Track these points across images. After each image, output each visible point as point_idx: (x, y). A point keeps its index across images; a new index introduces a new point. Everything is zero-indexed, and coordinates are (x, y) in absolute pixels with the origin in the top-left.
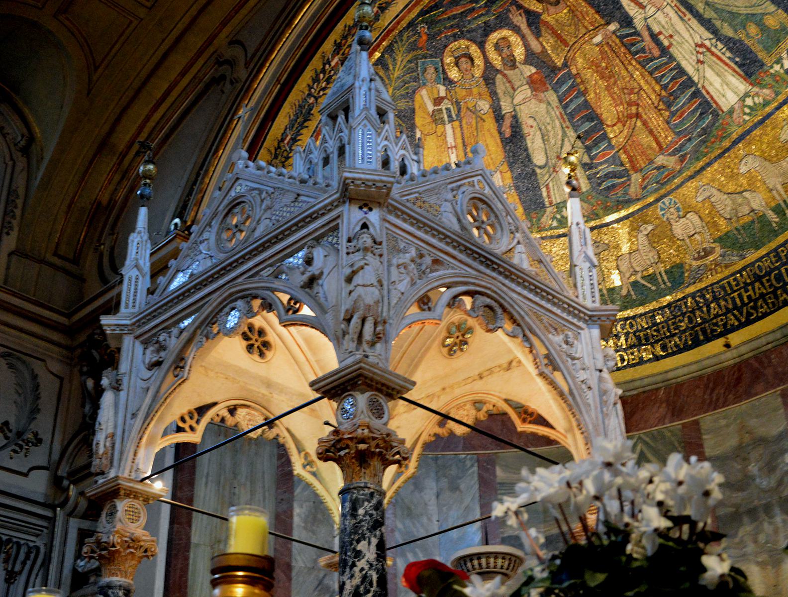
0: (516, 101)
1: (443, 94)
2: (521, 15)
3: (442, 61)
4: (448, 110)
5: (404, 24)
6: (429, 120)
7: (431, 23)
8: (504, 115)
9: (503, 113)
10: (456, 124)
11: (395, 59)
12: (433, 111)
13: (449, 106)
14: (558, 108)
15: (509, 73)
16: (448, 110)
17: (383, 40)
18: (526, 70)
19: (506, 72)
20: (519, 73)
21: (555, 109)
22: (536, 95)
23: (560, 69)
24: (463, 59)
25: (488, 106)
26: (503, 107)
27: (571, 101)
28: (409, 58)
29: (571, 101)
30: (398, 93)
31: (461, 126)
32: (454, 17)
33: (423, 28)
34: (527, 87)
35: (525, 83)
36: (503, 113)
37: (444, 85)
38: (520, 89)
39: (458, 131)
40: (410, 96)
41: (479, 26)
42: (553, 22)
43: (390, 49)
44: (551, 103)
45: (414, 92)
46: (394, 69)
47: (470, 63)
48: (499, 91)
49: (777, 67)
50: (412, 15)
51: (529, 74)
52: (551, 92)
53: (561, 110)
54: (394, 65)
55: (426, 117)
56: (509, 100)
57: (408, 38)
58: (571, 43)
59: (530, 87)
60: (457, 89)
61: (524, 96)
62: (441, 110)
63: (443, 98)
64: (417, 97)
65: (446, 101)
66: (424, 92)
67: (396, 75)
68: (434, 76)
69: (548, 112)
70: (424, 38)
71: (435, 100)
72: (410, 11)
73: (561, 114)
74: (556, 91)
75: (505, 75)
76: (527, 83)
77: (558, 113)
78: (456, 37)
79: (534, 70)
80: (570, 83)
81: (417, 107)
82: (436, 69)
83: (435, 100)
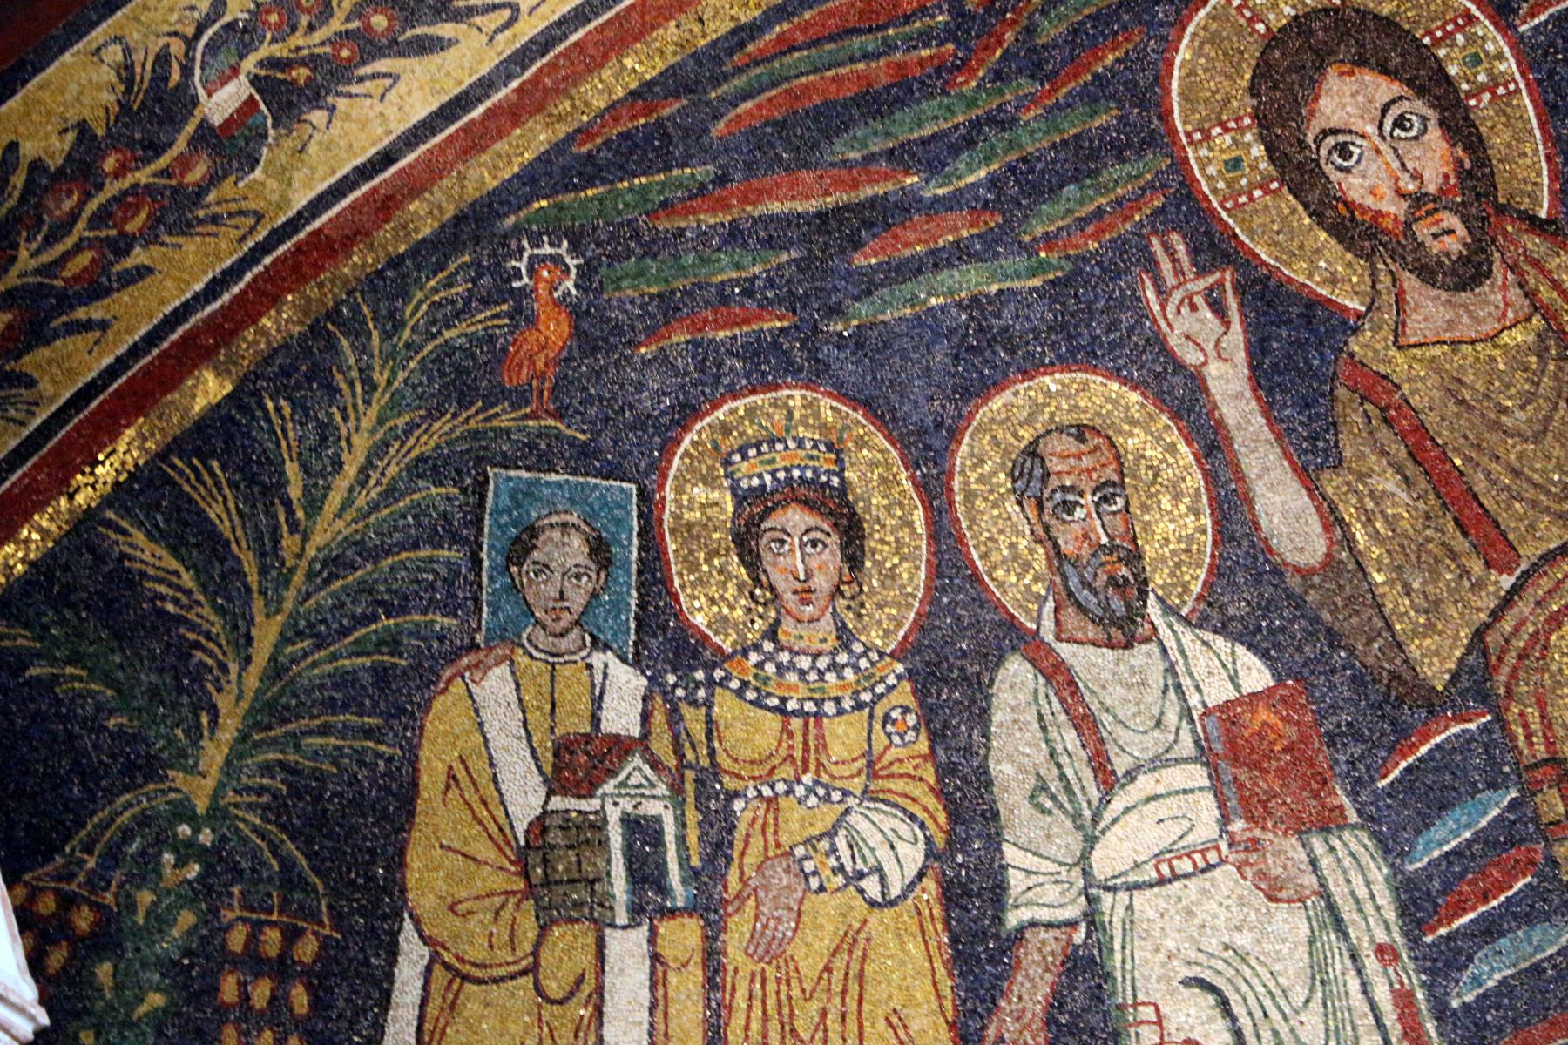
0: (1110, 858)
1: (621, 717)
2: (1218, 308)
3: (649, 503)
4: (641, 830)
6: (498, 878)
8: (1019, 935)
9: (1013, 919)
10: (684, 936)
11: (326, 433)
12: (540, 825)
13: (653, 808)
14: (1384, 952)
15: (1089, 662)
16: (641, 830)
18: (1201, 662)
19: (1065, 650)
20: (1156, 678)
21: (1371, 964)
22: (1254, 845)
23: (1434, 705)
24: (795, 519)
25: (913, 856)
26: (1016, 880)
27: (1488, 930)
28: (425, 443)
29: (1488, 930)
30: (316, 667)
31: (712, 960)
32: (774, 233)
34: (1198, 776)
35: (1187, 746)
36: (1013, 919)
37: (637, 663)
38: (1145, 784)
39: (687, 986)
41: (927, 325)
42: (1421, 390)
44: (1348, 913)
46: (314, 504)
47: (829, 559)
48: (1002, 768)
51: (1219, 692)
52: (1357, 842)
53: (1414, 981)
55: (485, 851)
56: (1067, 842)
58: (1530, 552)
59: (1217, 789)
60: (725, 706)
61: (1167, 835)
62: (600, 826)
63: (621, 747)
65: (635, 769)
66: (496, 686)
67: (327, 531)
68: (577, 600)
69: (1319, 975)
71: (563, 749)
73: (1404, 1000)
74: (1390, 847)
75: (1058, 676)
76: (1204, 755)
77: (1382, 994)
79: (1256, 675)
80: (1493, 807)
81: (430, 782)
82: (600, 551)
83: (563, 749)
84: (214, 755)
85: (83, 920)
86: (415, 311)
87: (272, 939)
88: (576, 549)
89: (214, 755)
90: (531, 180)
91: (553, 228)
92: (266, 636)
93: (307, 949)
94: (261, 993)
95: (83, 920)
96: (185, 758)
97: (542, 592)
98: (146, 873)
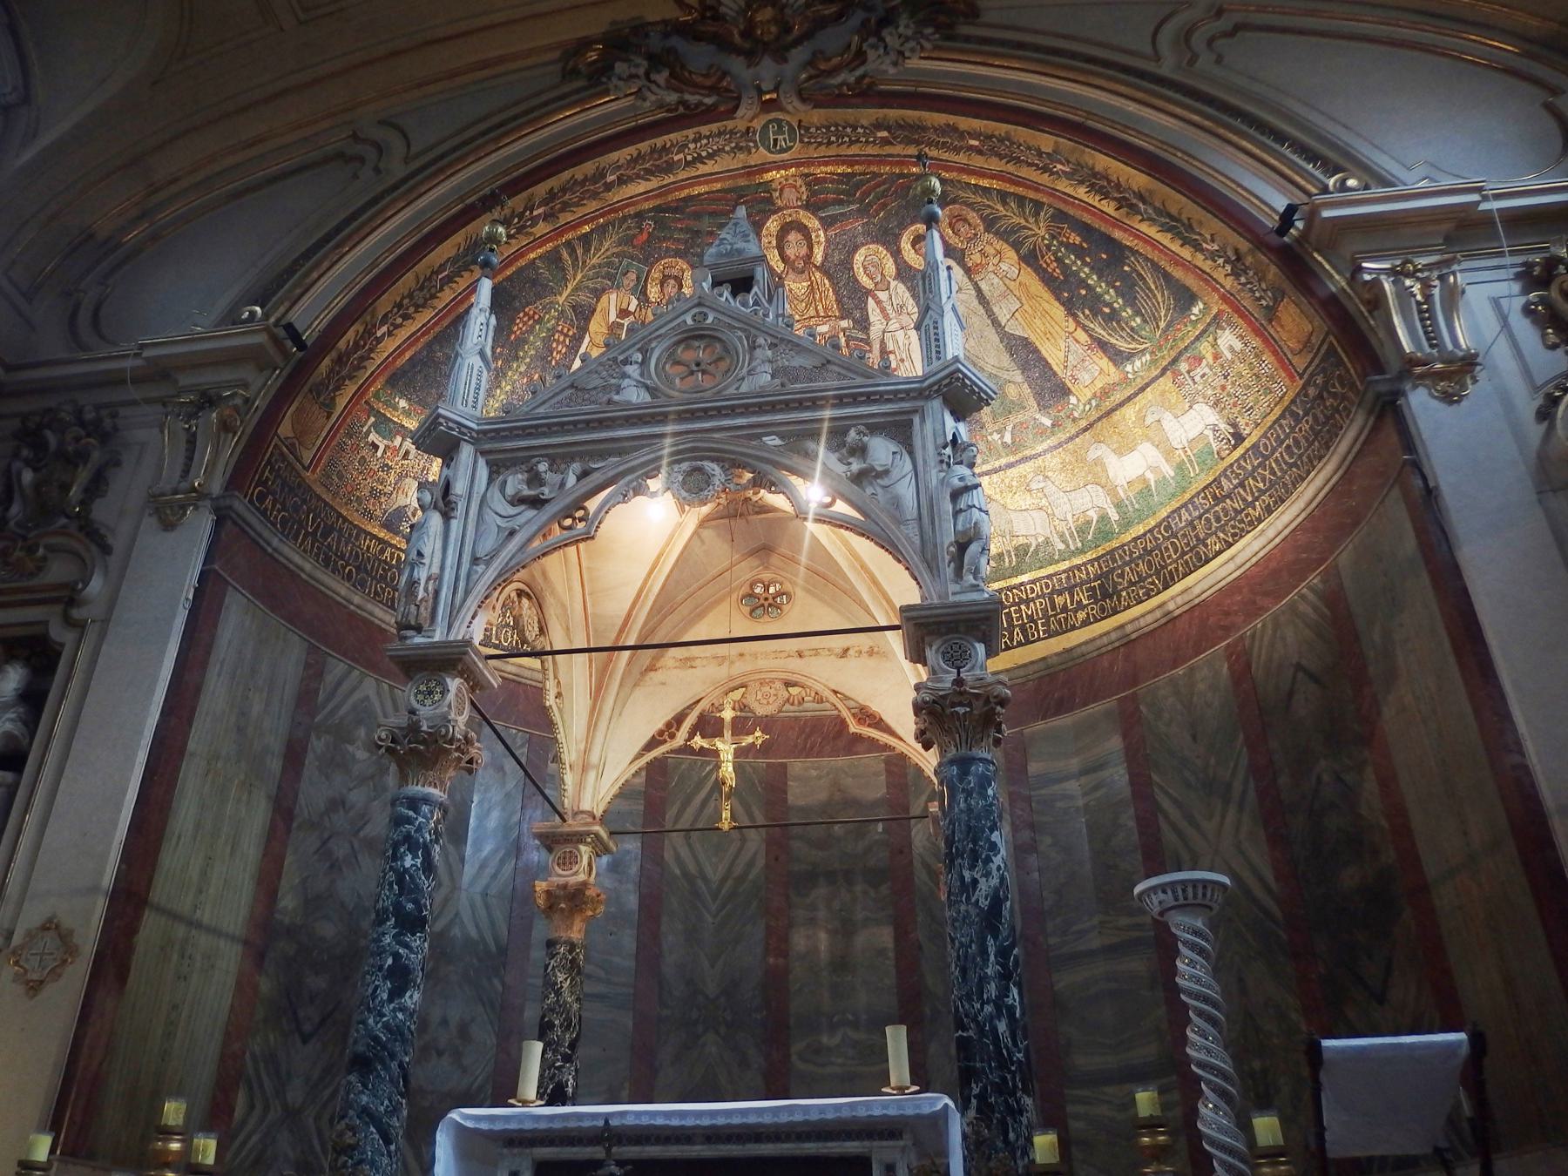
3: (649, 272)
5: (632, 210)
7: (661, 224)
11: (601, 244)
17: (602, 216)
28: (615, 250)
33: (649, 225)
40: (598, 293)
43: (602, 230)
45: (604, 290)
46: (594, 255)
49: (996, 436)
50: (646, 206)
54: (599, 250)
57: (629, 228)
64: (604, 298)
66: (613, 297)
67: (595, 261)
68: (632, 285)
70: (645, 236)
72: (647, 199)
78: (678, 254)
81: (598, 309)
82: (638, 278)
84: (565, 295)
85: (536, 317)
86: (624, 227)
87: (565, 330)
88: (634, 277)
89: (565, 295)
90: (650, 210)
91: (651, 218)
92: (579, 277)
93: (571, 333)
94: (562, 338)
95: (536, 317)
96: (561, 294)
97: (626, 282)
98: (548, 312)
